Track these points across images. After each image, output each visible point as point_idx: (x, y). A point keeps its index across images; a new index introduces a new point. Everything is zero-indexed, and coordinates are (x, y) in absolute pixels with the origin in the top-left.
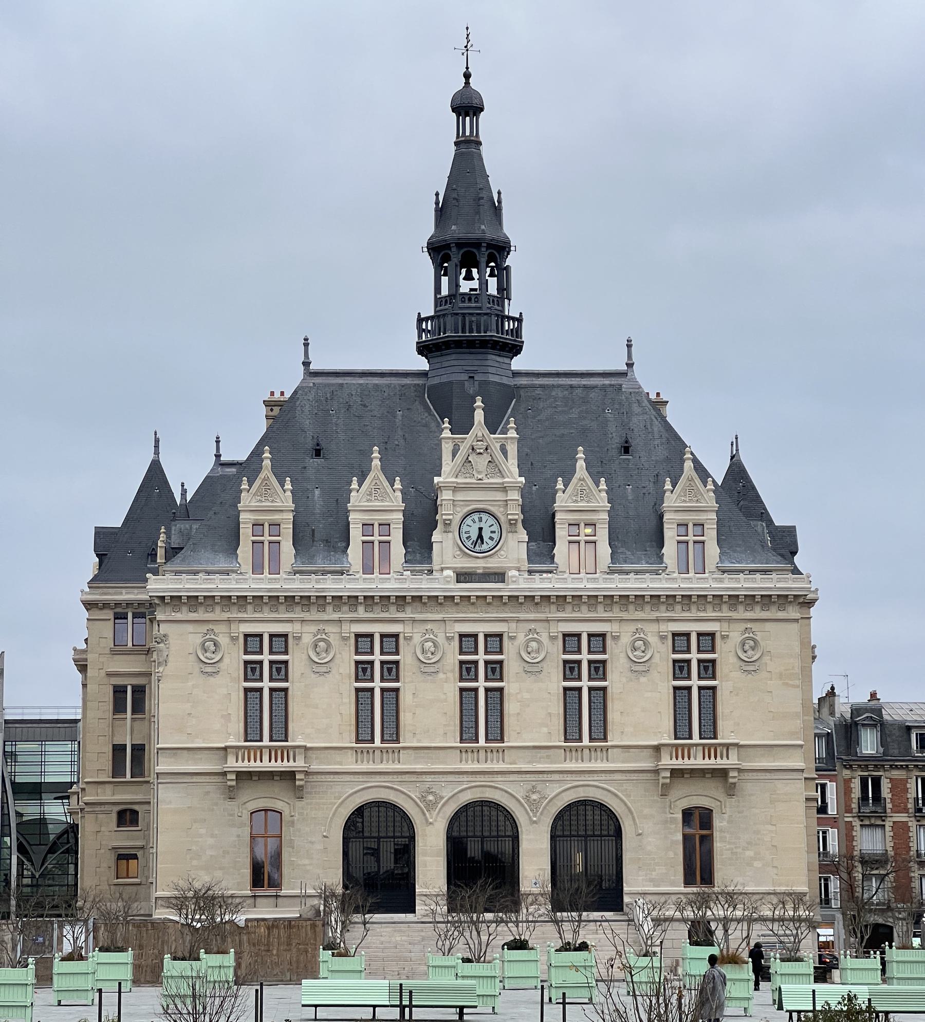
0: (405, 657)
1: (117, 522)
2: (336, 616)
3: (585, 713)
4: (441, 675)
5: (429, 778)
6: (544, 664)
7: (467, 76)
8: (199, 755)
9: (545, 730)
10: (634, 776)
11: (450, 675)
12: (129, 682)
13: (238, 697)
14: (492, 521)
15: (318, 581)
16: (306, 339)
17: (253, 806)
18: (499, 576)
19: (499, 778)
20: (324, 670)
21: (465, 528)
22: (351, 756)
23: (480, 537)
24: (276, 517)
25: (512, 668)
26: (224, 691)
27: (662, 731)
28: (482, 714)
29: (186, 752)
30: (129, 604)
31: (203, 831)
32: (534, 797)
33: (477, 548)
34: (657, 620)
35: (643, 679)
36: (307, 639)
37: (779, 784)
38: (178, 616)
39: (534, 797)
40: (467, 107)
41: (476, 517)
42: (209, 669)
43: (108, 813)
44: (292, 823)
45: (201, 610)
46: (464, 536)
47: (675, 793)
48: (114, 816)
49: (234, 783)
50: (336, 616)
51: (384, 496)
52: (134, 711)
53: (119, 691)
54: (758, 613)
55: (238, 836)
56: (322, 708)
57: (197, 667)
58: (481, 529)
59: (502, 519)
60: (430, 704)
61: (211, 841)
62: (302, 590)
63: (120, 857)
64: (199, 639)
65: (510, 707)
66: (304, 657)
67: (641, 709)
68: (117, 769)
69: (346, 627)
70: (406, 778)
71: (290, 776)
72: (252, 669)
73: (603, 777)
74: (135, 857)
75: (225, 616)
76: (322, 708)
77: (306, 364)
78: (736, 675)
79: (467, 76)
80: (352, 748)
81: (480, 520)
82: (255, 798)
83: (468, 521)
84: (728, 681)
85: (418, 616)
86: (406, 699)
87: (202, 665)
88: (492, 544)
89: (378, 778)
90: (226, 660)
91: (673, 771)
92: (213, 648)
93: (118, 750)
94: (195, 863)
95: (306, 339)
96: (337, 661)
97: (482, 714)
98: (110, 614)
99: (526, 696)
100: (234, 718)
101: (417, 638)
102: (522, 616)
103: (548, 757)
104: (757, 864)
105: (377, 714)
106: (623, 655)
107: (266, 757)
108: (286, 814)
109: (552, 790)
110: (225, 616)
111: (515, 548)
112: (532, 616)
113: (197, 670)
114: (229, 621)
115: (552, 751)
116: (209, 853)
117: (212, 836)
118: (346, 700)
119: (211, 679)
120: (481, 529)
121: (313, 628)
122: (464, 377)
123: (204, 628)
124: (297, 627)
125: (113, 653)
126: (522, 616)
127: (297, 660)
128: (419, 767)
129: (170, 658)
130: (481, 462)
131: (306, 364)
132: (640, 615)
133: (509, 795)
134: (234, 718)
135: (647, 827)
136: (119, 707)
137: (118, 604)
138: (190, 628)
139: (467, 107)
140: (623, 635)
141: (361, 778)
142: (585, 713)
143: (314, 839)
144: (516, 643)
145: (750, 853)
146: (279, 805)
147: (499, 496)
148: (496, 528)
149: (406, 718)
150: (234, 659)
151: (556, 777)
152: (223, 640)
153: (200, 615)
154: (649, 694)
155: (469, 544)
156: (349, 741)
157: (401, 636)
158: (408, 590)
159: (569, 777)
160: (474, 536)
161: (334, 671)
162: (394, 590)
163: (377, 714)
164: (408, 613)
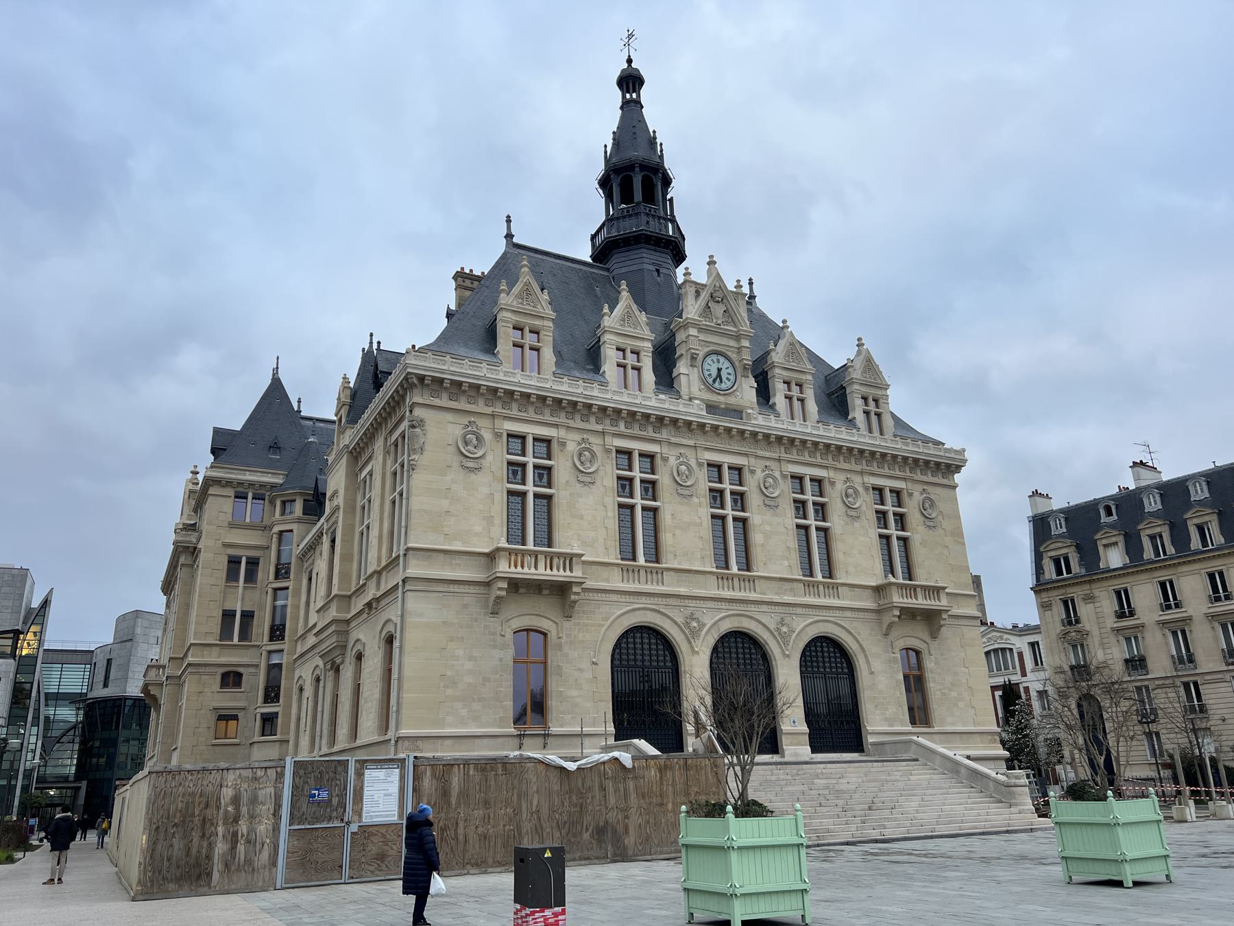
0: (663, 478)
1: (236, 423)
2: (599, 428)
3: (816, 551)
4: (695, 500)
5: (692, 603)
6: (780, 500)
7: (629, 61)
8: (457, 560)
9: (786, 563)
10: (861, 615)
11: (703, 500)
12: (244, 554)
13: (501, 498)
14: (727, 364)
15: (585, 388)
16: (508, 217)
17: (517, 623)
18: (737, 413)
19: (752, 608)
20: (589, 480)
21: (706, 366)
22: (617, 573)
23: (719, 376)
24: (537, 322)
25: (754, 500)
26: (485, 490)
27: (874, 574)
28: (733, 542)
29: (441, 556)
30: (251, 484)
31: (461, 652)
32: (785, 629)
33: (717, 385)
34: (862, 473)
35: (856, 524)
36: (572, 447)
37: (965, 629)
38: (437, 402)
39: (785, 629)
40: (630, 81)
41: (714, 357)
42: (470, 464)
43: (213, 674)
44: (560, 647)
45: (463, 399)
46: (707, 373)
47: (894, 634)
48: (219, 678)
49: (504, 593)
50: (599, 428)
51: (636, 324)
52: (246, 581)
53: (234, 562)
54: (929, 478)
55: (501, 660)
56: (587, 521)
57: (456, 460)
58: (719, 370)
59: (737, 364)
60: (687, 527)
61: (469, 665)
62: (571, 394)
63: (221, 718)
64: (458, 431)
65: (756, 538)
66: (569, 464)
67: (859, 554)
68: (226, 632)
69: (608, 439)
70: (671, 601)
71: (561, 590)
72: (516, 470)
73: (838, 613)
74: (235, 718)
75: (489, 410)
76: (587, 521)
77: (509, 236)
78: (921, 528)
79: (629, 61)
80: (618, 565)
81: (718, 361)
82: (522, 615)
83: (709, 360)
84: (917, 532)
85: (673, 440)
86: (666, 518)
87: (462, 458)
88: (729, 384)
89: (643, 600)
90: (489, 458)
91: (902, 609)
92: (475, 442)
93: (228, 615)
94: (449, 692)
95: (508, 217)
96: (601, 473)
97: (733, 542)
98: (230, 492)
99: (768, 528)
100: (497, 521)
101: (673, 461)
102: (760, 453)
103: (792, 590)
104: (961, 704)
105: (640, 534)
106: (839, 500)
107: (541, 565)
108: (552, 636)
109: (799, 624)
110: (489, 410)
111: (747, 392)
112: (767, 454)
113: (456, 465)
114: (493, 416)
115: (795, 585)
116: (469, 679)
117: (471, 658)
118: (610, 514)
119: (473, 476)
120: (719, 370)
121: (577, 437)
122: (652, 268)
123: (465, 420)
124: (562, 433)
125: (232, 526)
126: (760, 453)
127: (562, 467)
128: (683, 590)
129: (427, 447)
130: (718, 310)
131: (509, 236)
132: (846, 466)
133: (760, 625)
134: (497, 521)
135: (877, 665)
136: (232, 575)
137: (240, 484)
138: (449, 417)
139: (630, 81)
140: (837, 481)
141: (628, 599)
142: (816, 551)
143: (582, 666)
144: (756, 477)
145: (954, 694)
146: (545, 625)
147: (732, 343)
148: (731, 370)
149: (667, 538)
150: (496, 457)
151: (799, 611)
152: (487, 435)
153: (463, 405)
154: (862, 539)
155: (710, 381)
156: (614, 558)
157: (659, 456)
158: (668, 410)
159: (810, 612)
160: (714, 373)
161: (598, 482)
162: (655, 408)
163: (640, 534)
164: (664, 434)
